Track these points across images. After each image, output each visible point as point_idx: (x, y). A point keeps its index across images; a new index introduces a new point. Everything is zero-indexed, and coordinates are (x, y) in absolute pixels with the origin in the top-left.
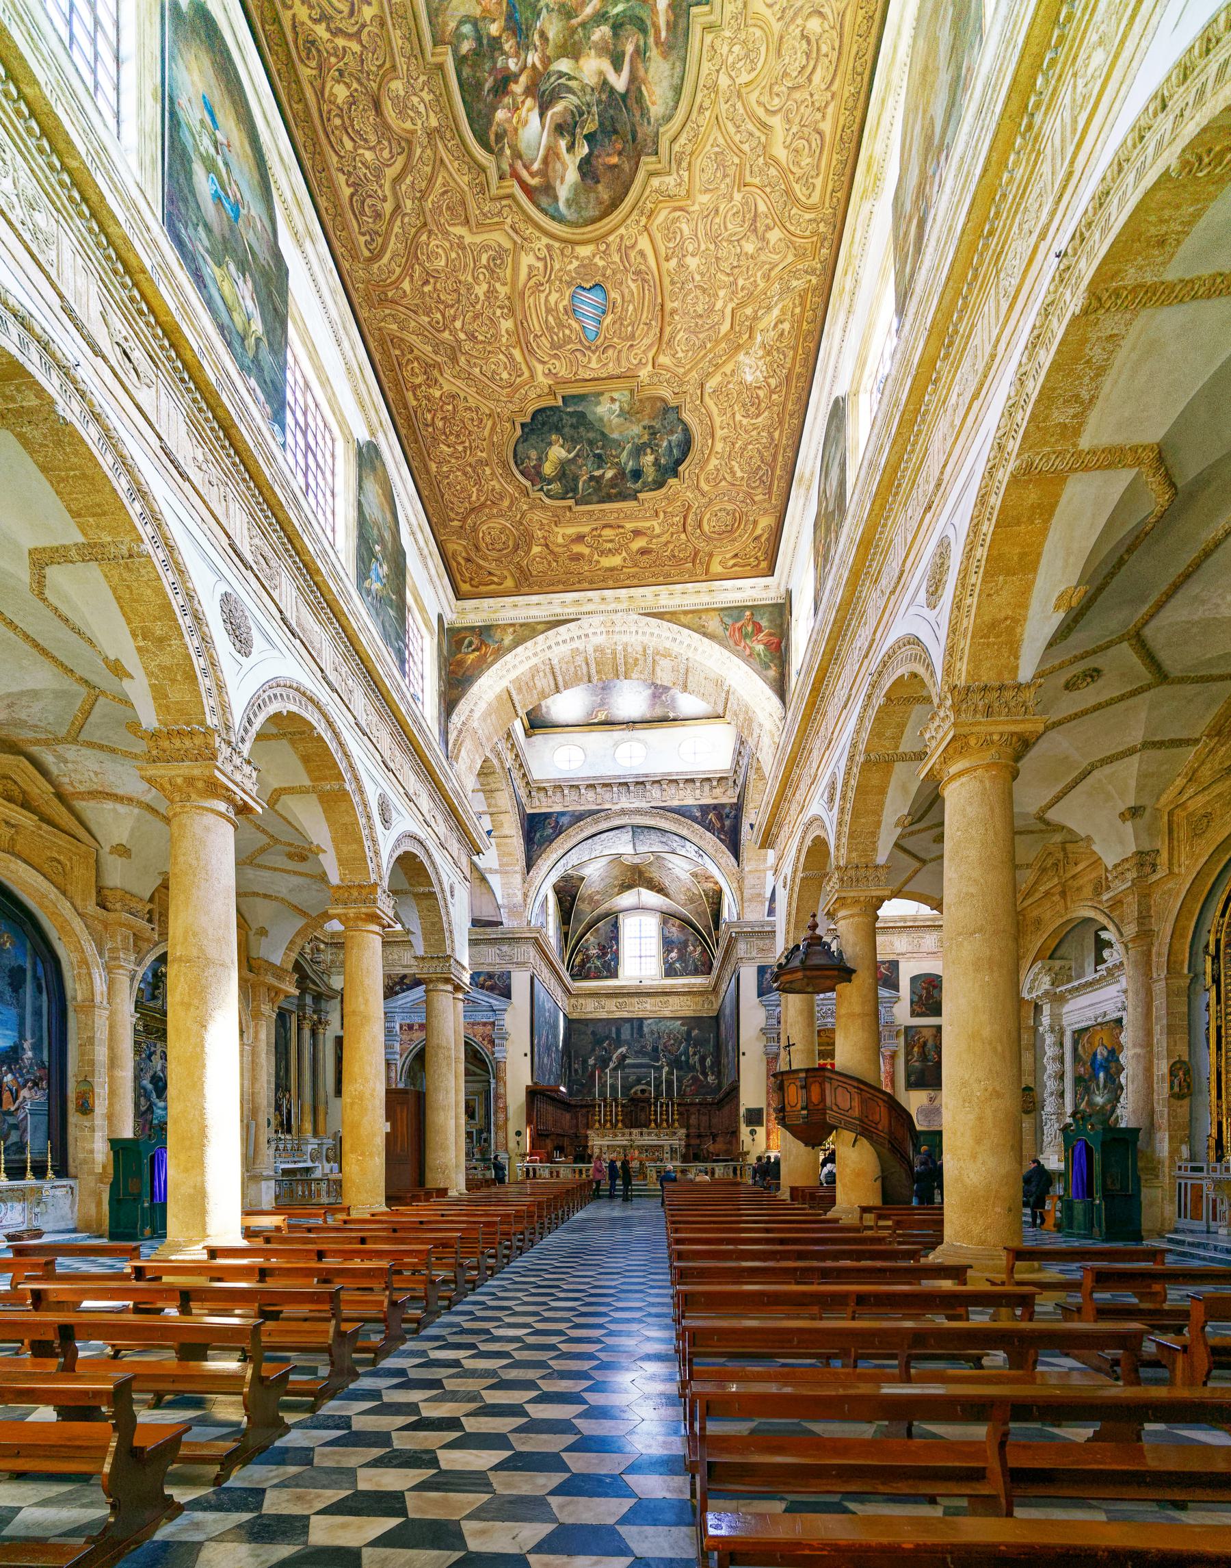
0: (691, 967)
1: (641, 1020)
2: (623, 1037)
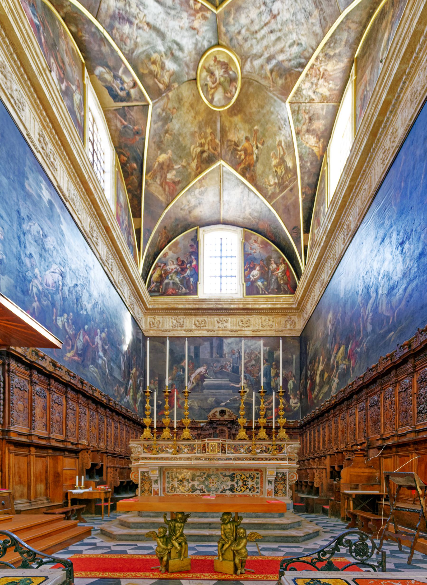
0: (273, 286)
1: (221, 339)
2: (202, 356)
